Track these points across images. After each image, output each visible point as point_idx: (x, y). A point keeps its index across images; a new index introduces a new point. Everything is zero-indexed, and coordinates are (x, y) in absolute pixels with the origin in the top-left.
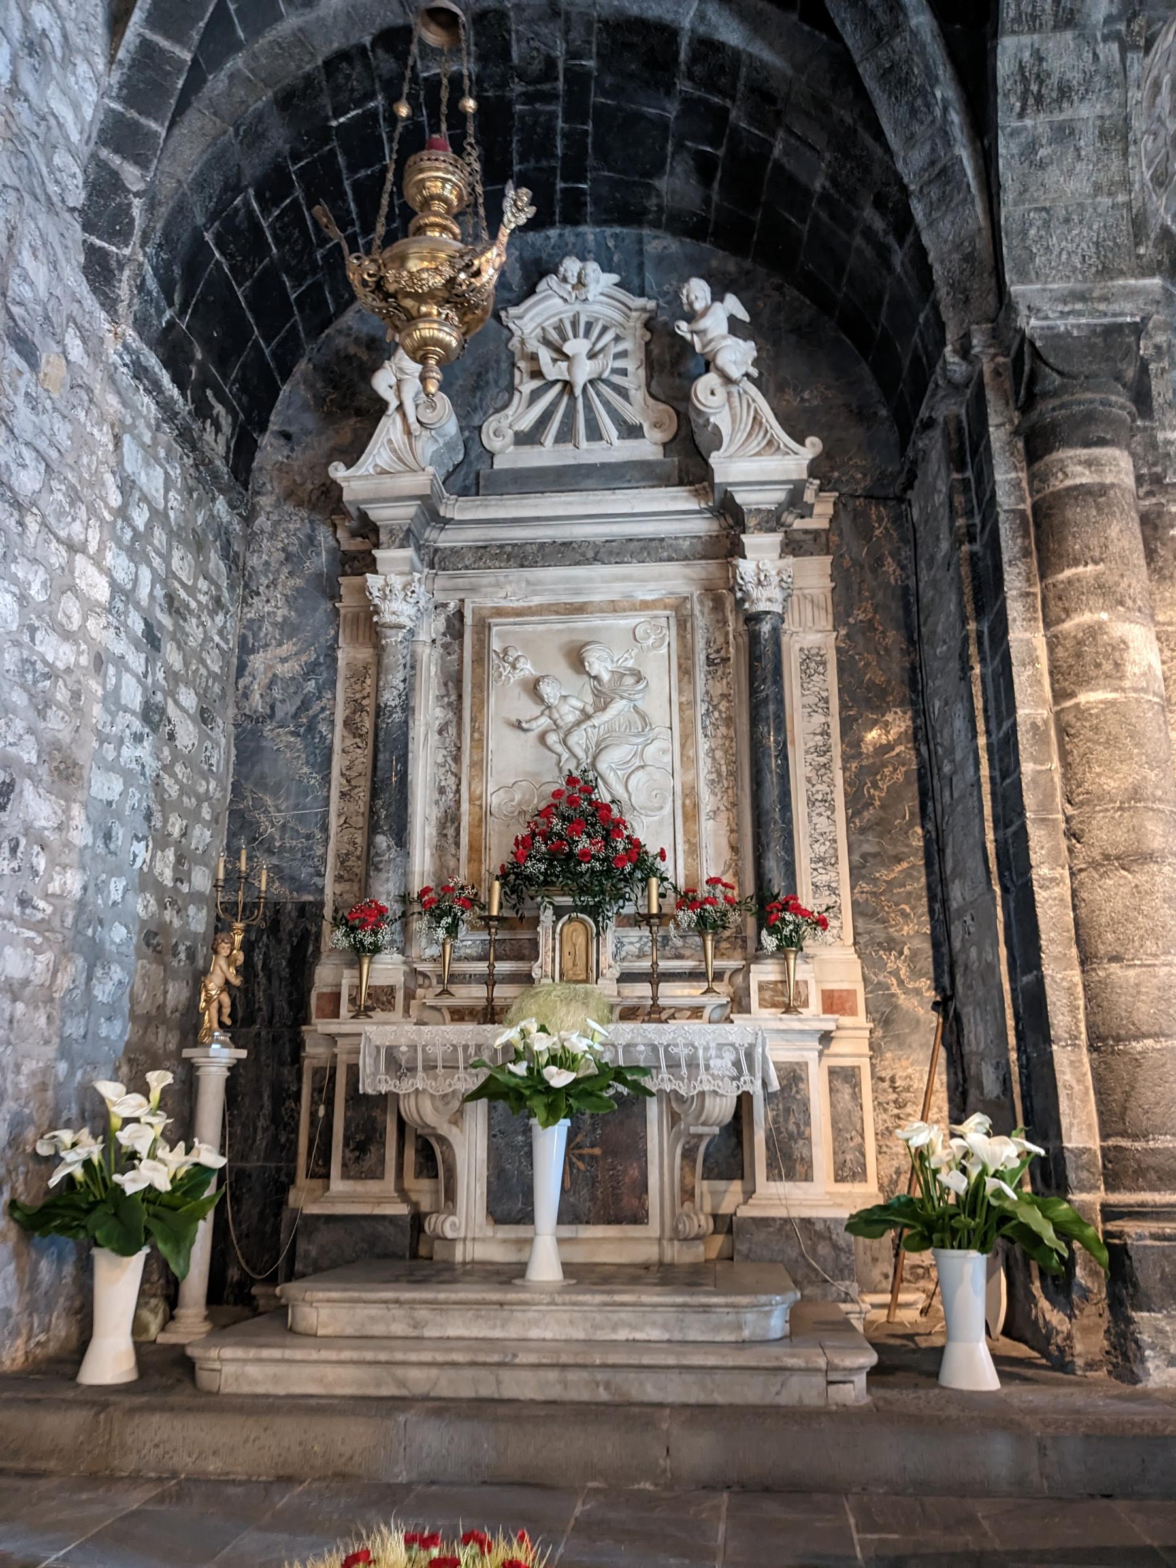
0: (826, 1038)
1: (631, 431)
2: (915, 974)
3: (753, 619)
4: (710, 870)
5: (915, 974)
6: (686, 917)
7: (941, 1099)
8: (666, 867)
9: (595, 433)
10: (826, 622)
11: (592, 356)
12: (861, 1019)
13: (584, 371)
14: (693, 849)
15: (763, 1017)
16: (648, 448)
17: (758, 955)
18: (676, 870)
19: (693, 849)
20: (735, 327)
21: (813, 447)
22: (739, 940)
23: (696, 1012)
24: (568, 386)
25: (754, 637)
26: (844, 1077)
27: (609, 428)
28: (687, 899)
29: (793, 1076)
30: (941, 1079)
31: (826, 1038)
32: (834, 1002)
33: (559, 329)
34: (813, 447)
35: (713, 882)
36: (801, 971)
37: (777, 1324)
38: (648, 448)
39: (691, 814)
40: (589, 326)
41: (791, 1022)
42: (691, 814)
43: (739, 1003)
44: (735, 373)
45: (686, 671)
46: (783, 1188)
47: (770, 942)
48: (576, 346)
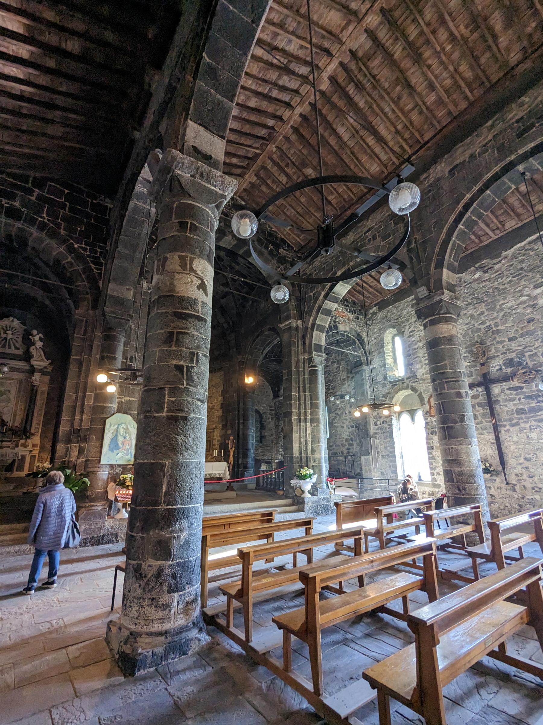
0: (31, 451)
1: (17, 348)
2: (49, 441)
3: (34, 386)
4: (16, 424)
5: (49, 441)
6: (10, 432)
7: (49, 460)
8: (8, 424)
9: (10, 347)
10: (47, 386)
11: (12, 334)
12: (38, 448)
13: (10, 337)
14: (14, 421)
15: (20, 448)
16: (20, 352)
17: (22, 439)
18: (10, 424)
19: (14, 421)
20: (41, 340)
21: (50, 361)
22: (19, 436)
23: (9, 447)
24: (6, 338)
25: (33, 389)
26: (33, 457)
27: (13, 348)
28: (11, 429)
29: (23, 457)
30: (50, 457)
31: (31, 451)
32: (34, 446)
33: (6, 327)
34: (50, 361)
35: (17, 427)
36: (29, 441)
37: (12, 488)
38: (20, 352)
39: (15, 416)
40: (13, 328)
41: (25, 449)
42: (15, 416)
43: (17, 446)
44: (38, 347)
45: (19, 391)
46: (18, 473)
47: (24, 437)
48: (9, 332)
